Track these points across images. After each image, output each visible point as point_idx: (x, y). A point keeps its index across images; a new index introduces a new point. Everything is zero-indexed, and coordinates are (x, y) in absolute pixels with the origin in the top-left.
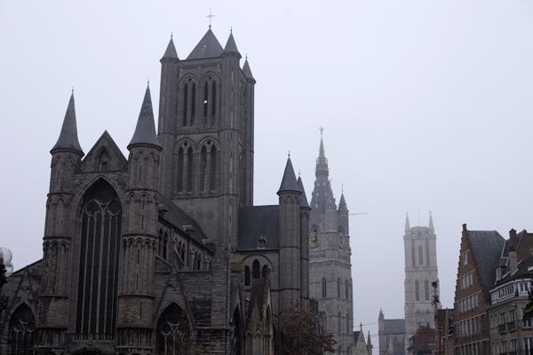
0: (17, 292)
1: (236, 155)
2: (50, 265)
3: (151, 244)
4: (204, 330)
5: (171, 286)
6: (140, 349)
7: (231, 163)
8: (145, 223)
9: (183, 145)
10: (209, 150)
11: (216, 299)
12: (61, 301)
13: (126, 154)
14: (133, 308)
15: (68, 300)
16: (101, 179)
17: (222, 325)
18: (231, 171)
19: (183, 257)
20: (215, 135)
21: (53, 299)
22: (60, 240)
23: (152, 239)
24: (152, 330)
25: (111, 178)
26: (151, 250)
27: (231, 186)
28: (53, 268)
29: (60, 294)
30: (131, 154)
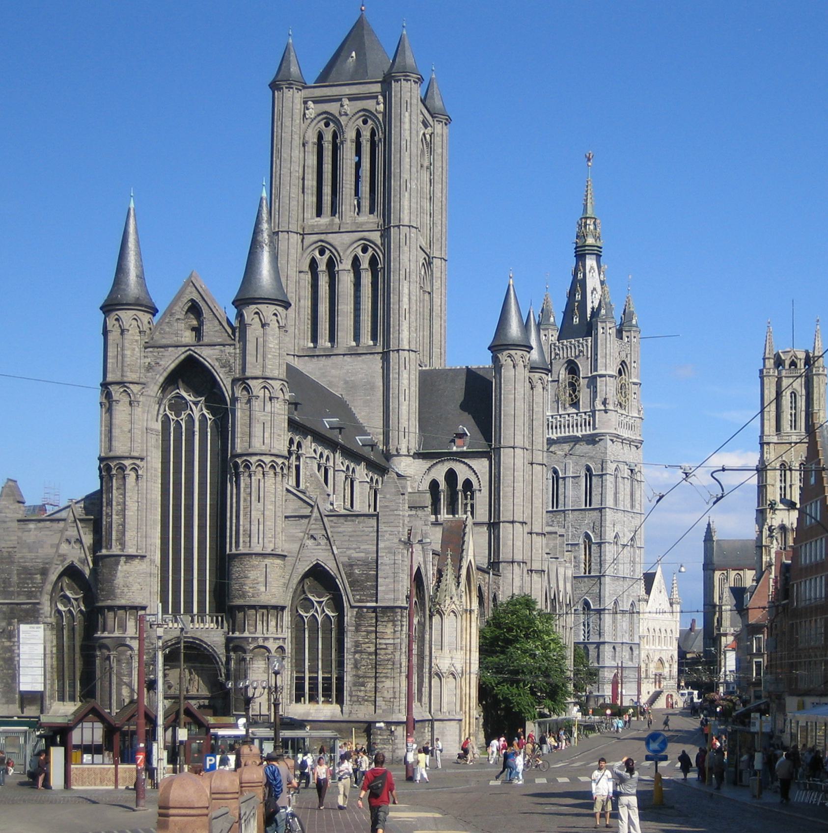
0: (58, 546)
1: (413, 276)
2: (114, 503)
3: (278, 470)
4: (365, 607)
5: (312, 536)
6: (265, 639)
7: (406, 291)
8: (267, 435)
9: (317, 253)
10: (365, 264)
11: (385, 559)
12: (137, 561)
13: (232, 313)
14: (252, 575)
15: (145, 560)
16: (190, 356)
17: (395, 600)
18: (406, 306)
19: (327, 484)
20: (376, 237)
21: (123, 559)
22: (127, 463)
23: (280, 461)
24: (283, 608)
25: (208, 356)
26: (279, 478)
27: (405, 335)
28: (120, 507)
29: (131, 551)
30: (240, 316)
